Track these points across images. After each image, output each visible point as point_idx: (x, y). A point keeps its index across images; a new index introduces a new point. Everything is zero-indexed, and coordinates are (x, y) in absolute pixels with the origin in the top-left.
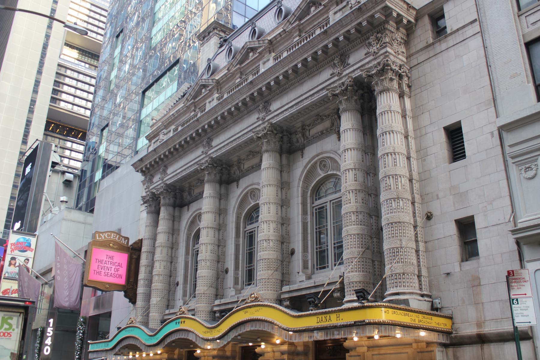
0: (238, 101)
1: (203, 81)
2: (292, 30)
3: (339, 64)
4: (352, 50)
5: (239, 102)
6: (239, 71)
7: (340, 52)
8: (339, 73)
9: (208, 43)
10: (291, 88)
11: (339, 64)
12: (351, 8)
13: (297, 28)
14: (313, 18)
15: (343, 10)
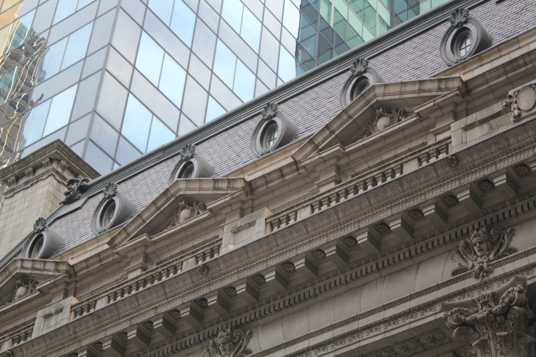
0: (154, 312)
1: (28, 265)
2: (316, 165)
3: (484, 246)
4: (522, 217)
5: (157, 317)
6: (143, 249)
7: (488, 218)
8: (481, 268)
9: (29, 190)
10: (320, 298)
11: (484, 246)
12: (518, 118)
13: (333, 162)
14: (383, 143)
15: (493, 122)
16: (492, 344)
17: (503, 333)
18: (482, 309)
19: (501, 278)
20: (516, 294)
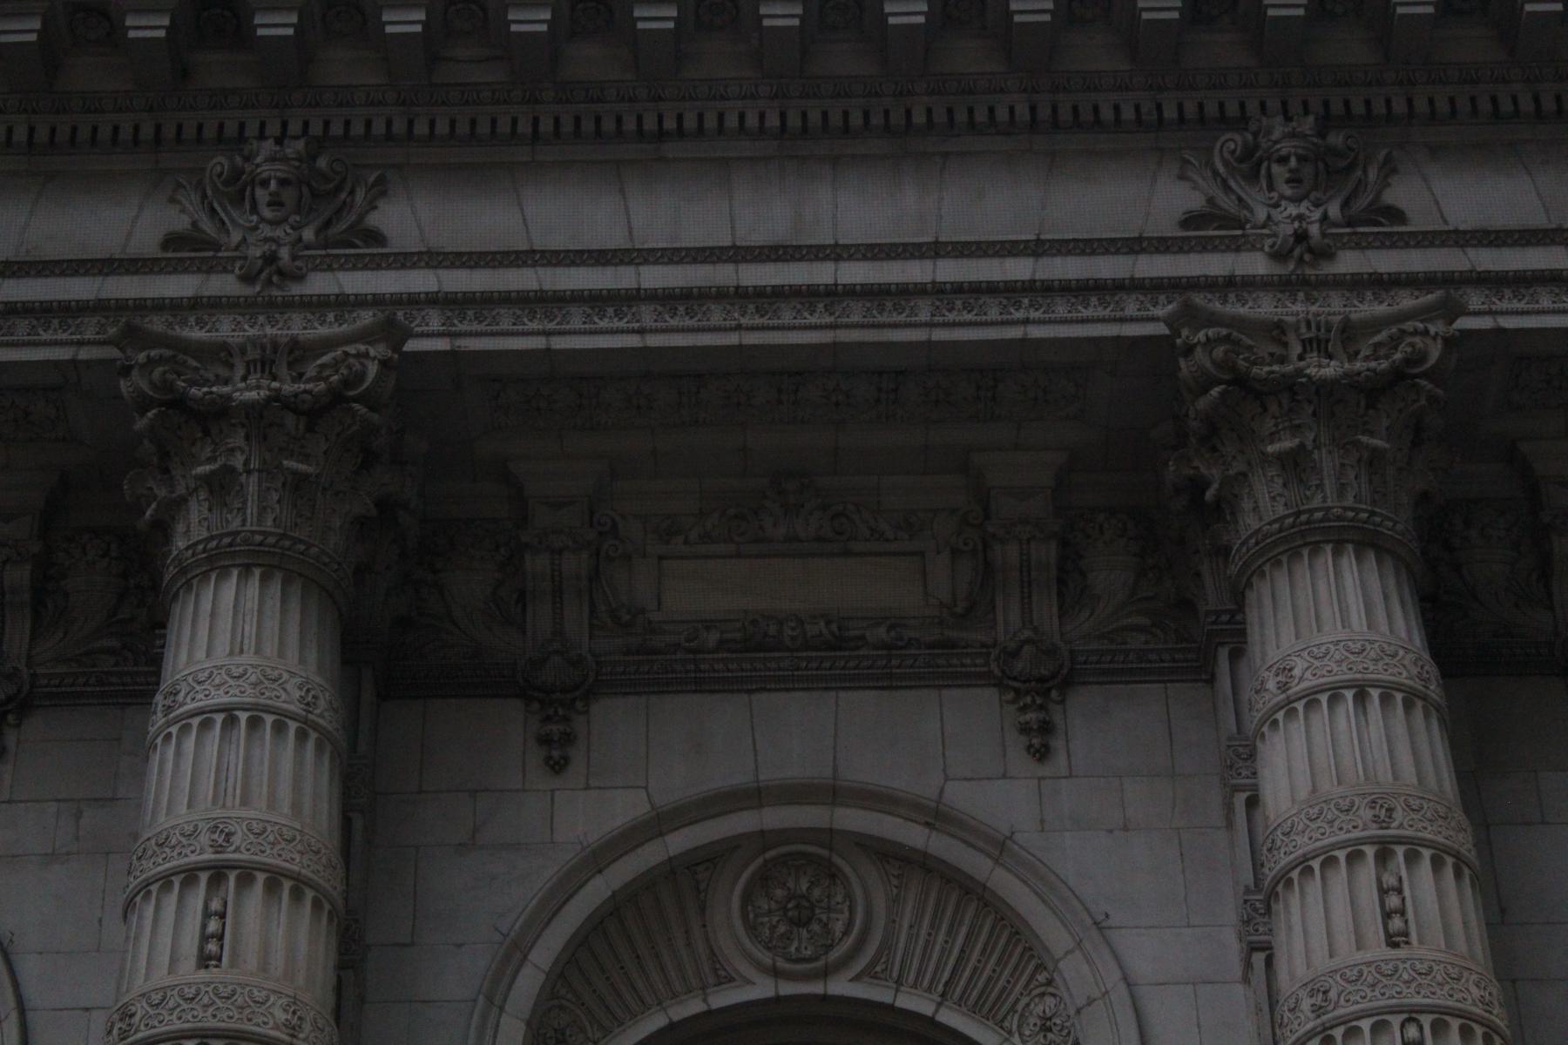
3: (289, 195)
11: (289, 195)
16: (252, 485)
17: (302, 467)
18: (244, 379)
19: (319, 305)
20: (372, 369)
